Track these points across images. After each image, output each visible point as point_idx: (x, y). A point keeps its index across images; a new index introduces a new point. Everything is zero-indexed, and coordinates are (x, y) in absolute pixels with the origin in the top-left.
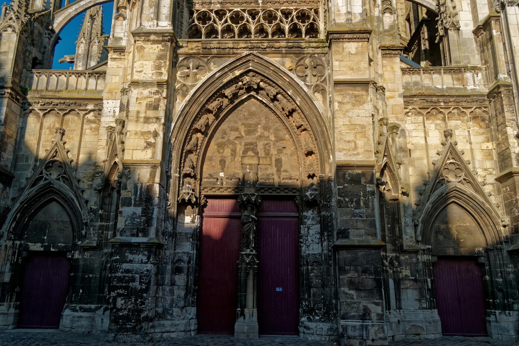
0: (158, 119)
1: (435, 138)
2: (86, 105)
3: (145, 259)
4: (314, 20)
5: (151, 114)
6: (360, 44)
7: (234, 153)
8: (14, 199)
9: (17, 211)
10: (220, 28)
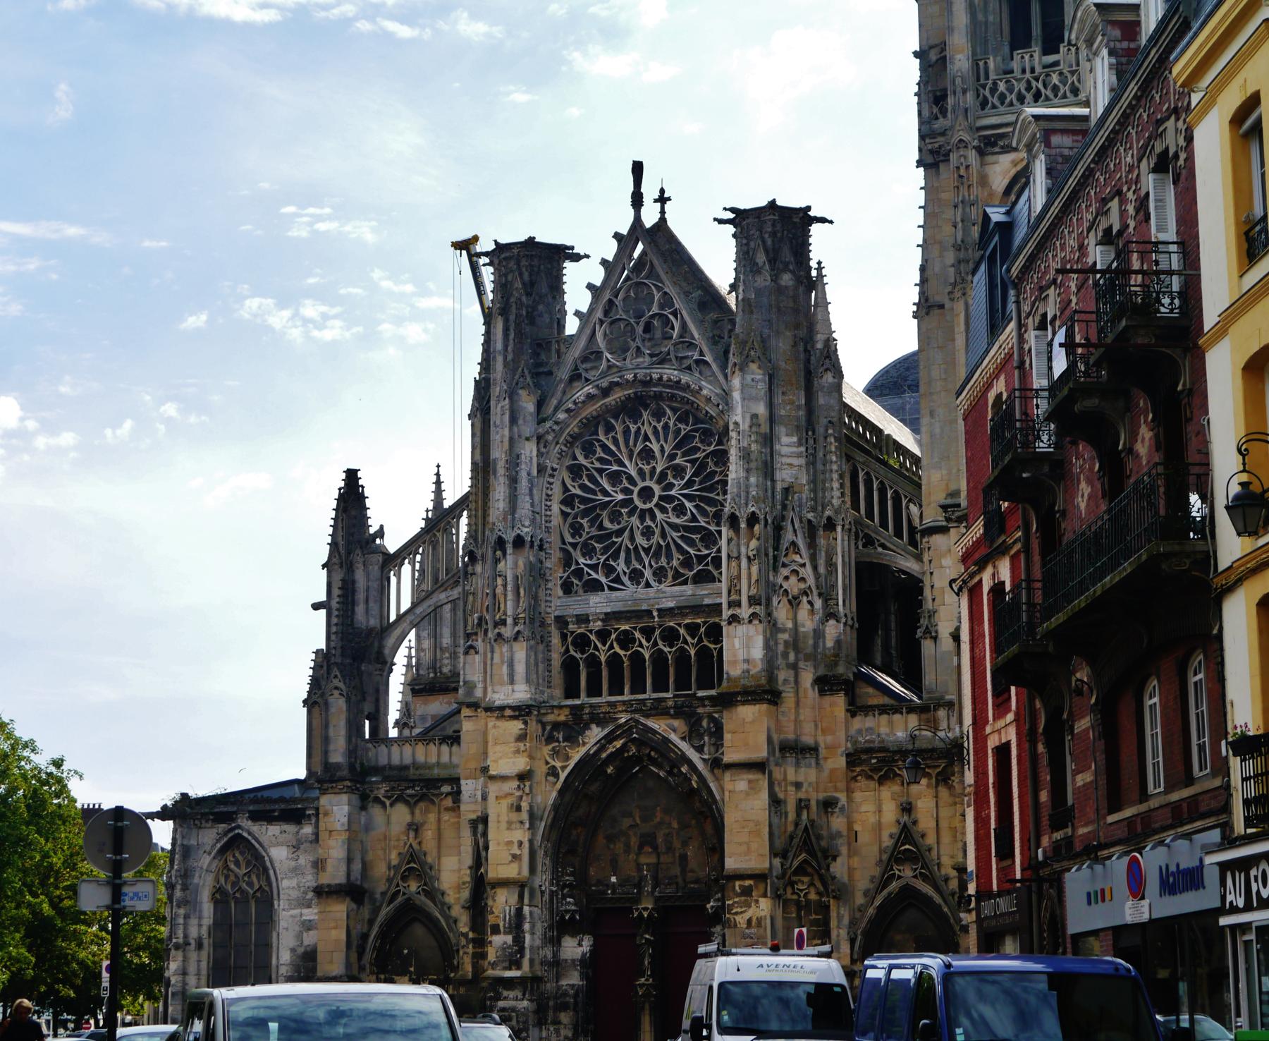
0: (521, 822)
1: (890, 812)
3: (520, 996)
5: (514, 816)
7: (628, 849)
8: (371, 922)
9: (376, 938)
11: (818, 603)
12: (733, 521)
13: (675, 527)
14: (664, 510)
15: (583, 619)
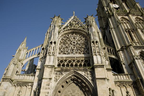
2: (29, 84)
4: (89, 62)
6: (102, 68)
10: (66, 64)
11: (105, 58)
12: (93, 42)
13: (79, 47)
14: (77, 45)
15: (63, 57)
